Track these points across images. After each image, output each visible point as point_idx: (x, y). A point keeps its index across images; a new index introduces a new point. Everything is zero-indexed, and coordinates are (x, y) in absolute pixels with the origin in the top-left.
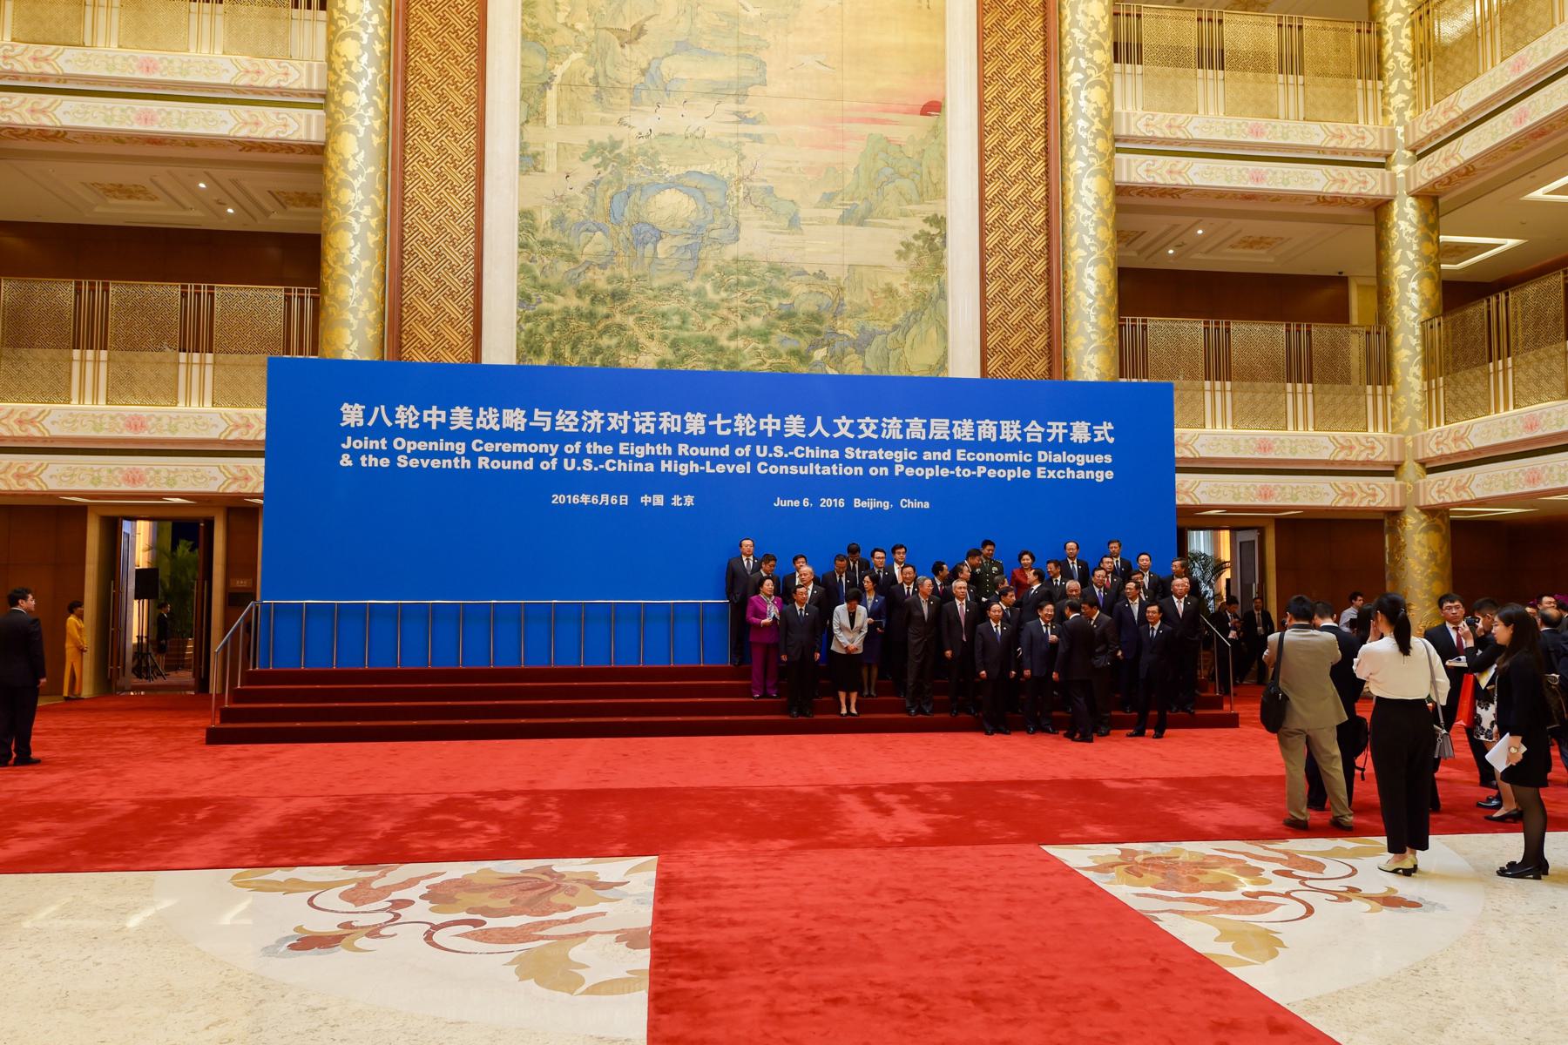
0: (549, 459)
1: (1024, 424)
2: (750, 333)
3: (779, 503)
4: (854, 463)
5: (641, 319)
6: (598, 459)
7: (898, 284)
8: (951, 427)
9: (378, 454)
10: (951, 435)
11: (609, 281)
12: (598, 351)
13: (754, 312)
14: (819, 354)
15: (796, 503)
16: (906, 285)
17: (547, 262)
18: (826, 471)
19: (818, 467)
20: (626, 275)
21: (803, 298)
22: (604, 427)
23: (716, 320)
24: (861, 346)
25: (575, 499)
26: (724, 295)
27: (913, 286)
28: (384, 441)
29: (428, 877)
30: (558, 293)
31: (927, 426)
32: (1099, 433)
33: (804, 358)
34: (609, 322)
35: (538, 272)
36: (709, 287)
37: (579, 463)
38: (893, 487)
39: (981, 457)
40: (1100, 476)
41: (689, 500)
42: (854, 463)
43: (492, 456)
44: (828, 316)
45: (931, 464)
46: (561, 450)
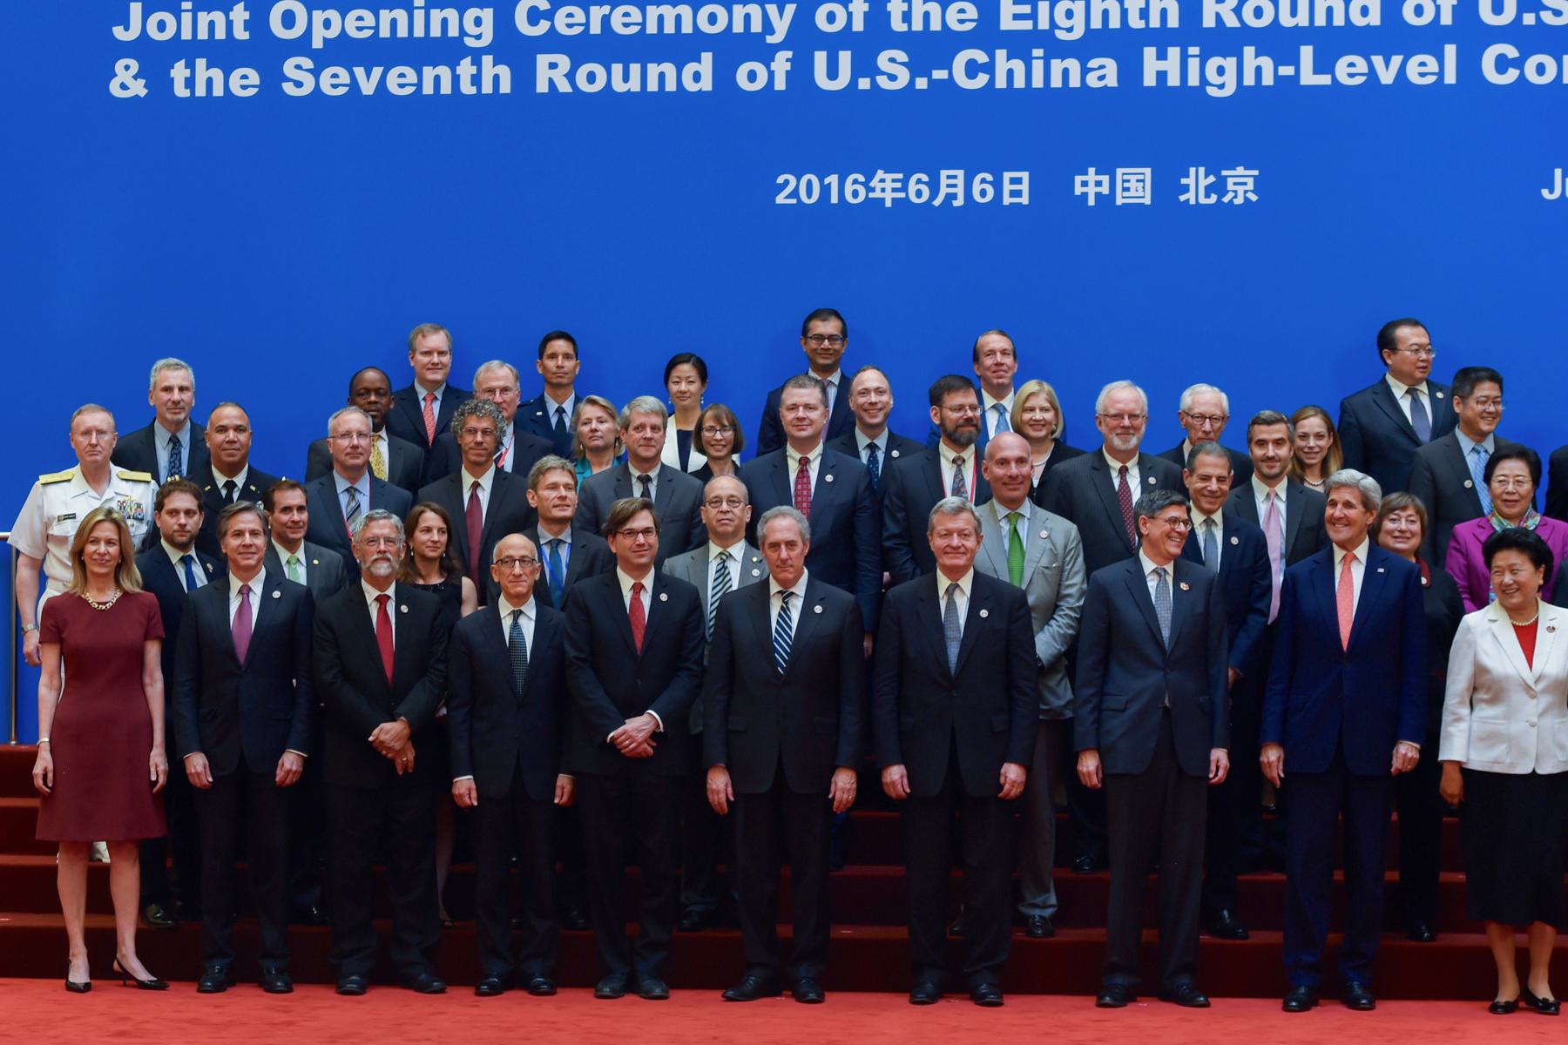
9: (224, 54)
25: (853, 190)
28: (240, 14)
37: (865, 66)
41: (1241, 184)
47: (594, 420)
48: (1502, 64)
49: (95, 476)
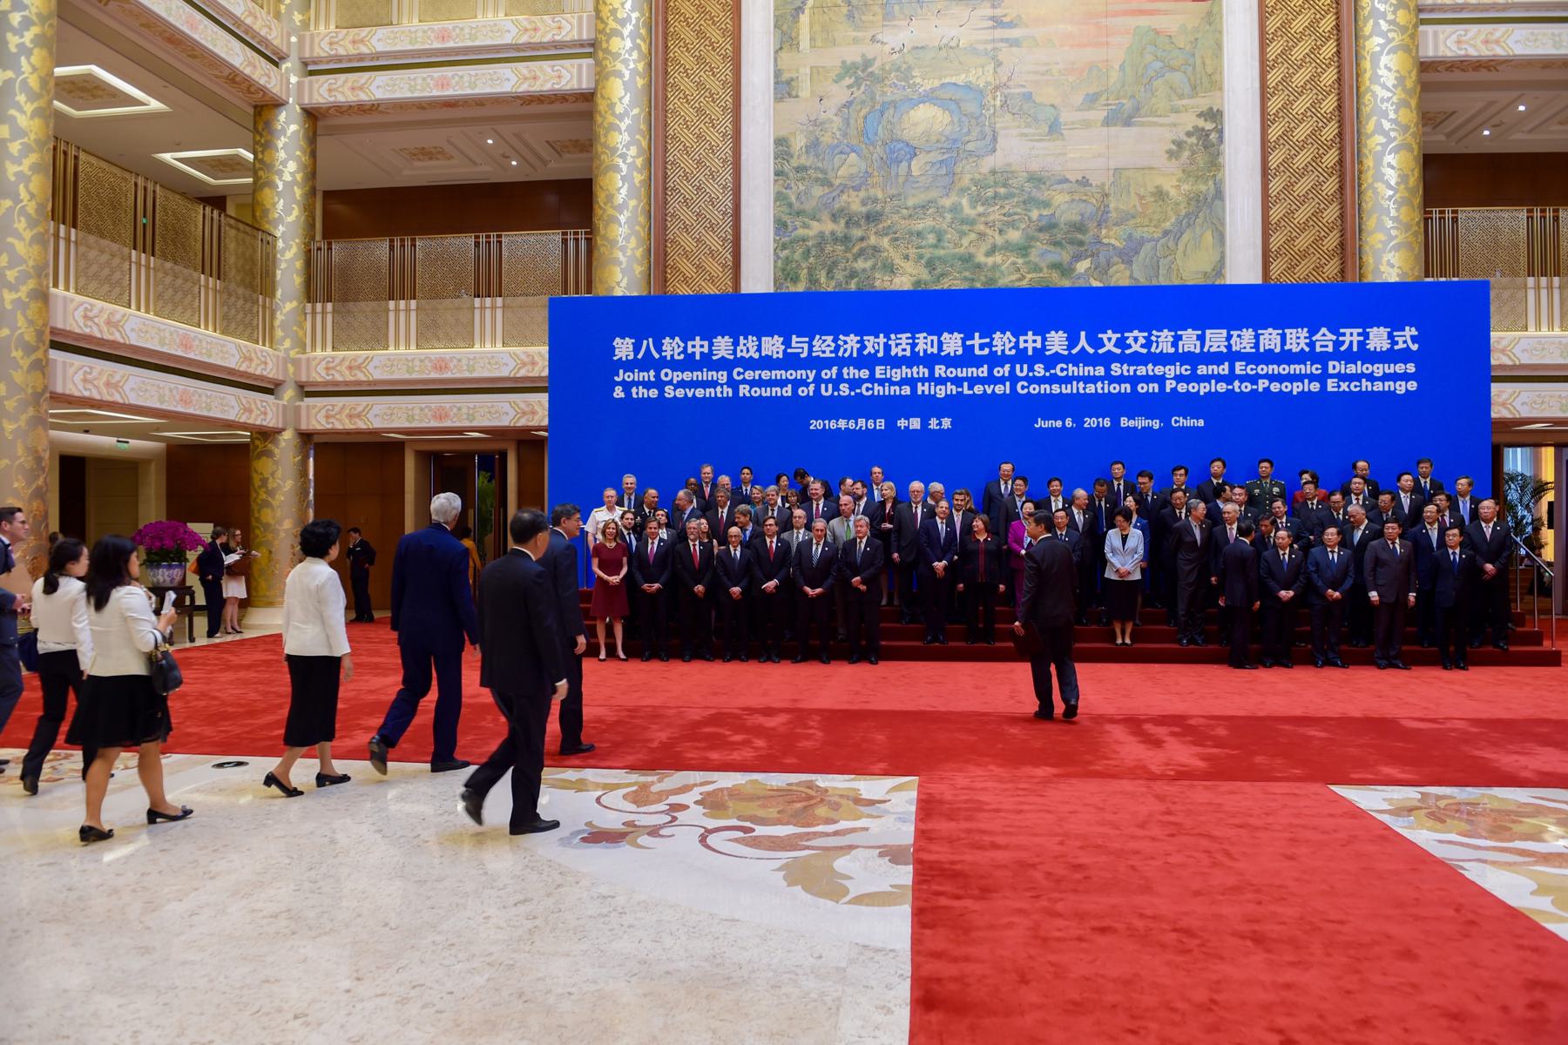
0: (807, 385)
1: (1313, 332)
2: (1008, 247)
3: (1040, 424)
4: (1121, 379)
5: (896, 239)
6: (855, 383)
7: (1168, 185)
8: (1229, 338)
10: (1229, 347)
11: (864, 203)
12: (853, 274)
13: (1012, 225)
14: (1082, 266)
15: (1059, 424)
16: (1178, 187)
17: (802, 188)
18: (1091, 389)
19: (1081, 385)
20: (880, 196)
21: (1063, 206)
22: (860, 350)
23: (973, 236)
24: (1127, 256)
25: (833, 425)
26: (980, 209)
27: (1186, 187)
28: (652, 373)
29: (702, 784)
30: (814, 218)
31: (1202, 338)
32: (1400, 340)
33: (1066, 270)
34: (864, 244)
35: (793, 199)
36: (965, 202)
37: (836, 388)
38: (1164, 404)
39: (1263, 369)
40: (1401, 388)
41: (947, 423)
42: (1121, 379)
43: (753, 383)
44: (1092, 225)
45: (1207, 378)
46: (818, 376)
47: (756, 492)
48: (1023, 387)
49: (611, 509)
